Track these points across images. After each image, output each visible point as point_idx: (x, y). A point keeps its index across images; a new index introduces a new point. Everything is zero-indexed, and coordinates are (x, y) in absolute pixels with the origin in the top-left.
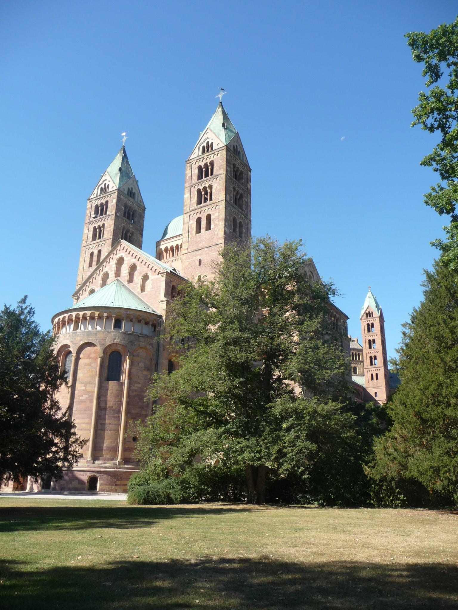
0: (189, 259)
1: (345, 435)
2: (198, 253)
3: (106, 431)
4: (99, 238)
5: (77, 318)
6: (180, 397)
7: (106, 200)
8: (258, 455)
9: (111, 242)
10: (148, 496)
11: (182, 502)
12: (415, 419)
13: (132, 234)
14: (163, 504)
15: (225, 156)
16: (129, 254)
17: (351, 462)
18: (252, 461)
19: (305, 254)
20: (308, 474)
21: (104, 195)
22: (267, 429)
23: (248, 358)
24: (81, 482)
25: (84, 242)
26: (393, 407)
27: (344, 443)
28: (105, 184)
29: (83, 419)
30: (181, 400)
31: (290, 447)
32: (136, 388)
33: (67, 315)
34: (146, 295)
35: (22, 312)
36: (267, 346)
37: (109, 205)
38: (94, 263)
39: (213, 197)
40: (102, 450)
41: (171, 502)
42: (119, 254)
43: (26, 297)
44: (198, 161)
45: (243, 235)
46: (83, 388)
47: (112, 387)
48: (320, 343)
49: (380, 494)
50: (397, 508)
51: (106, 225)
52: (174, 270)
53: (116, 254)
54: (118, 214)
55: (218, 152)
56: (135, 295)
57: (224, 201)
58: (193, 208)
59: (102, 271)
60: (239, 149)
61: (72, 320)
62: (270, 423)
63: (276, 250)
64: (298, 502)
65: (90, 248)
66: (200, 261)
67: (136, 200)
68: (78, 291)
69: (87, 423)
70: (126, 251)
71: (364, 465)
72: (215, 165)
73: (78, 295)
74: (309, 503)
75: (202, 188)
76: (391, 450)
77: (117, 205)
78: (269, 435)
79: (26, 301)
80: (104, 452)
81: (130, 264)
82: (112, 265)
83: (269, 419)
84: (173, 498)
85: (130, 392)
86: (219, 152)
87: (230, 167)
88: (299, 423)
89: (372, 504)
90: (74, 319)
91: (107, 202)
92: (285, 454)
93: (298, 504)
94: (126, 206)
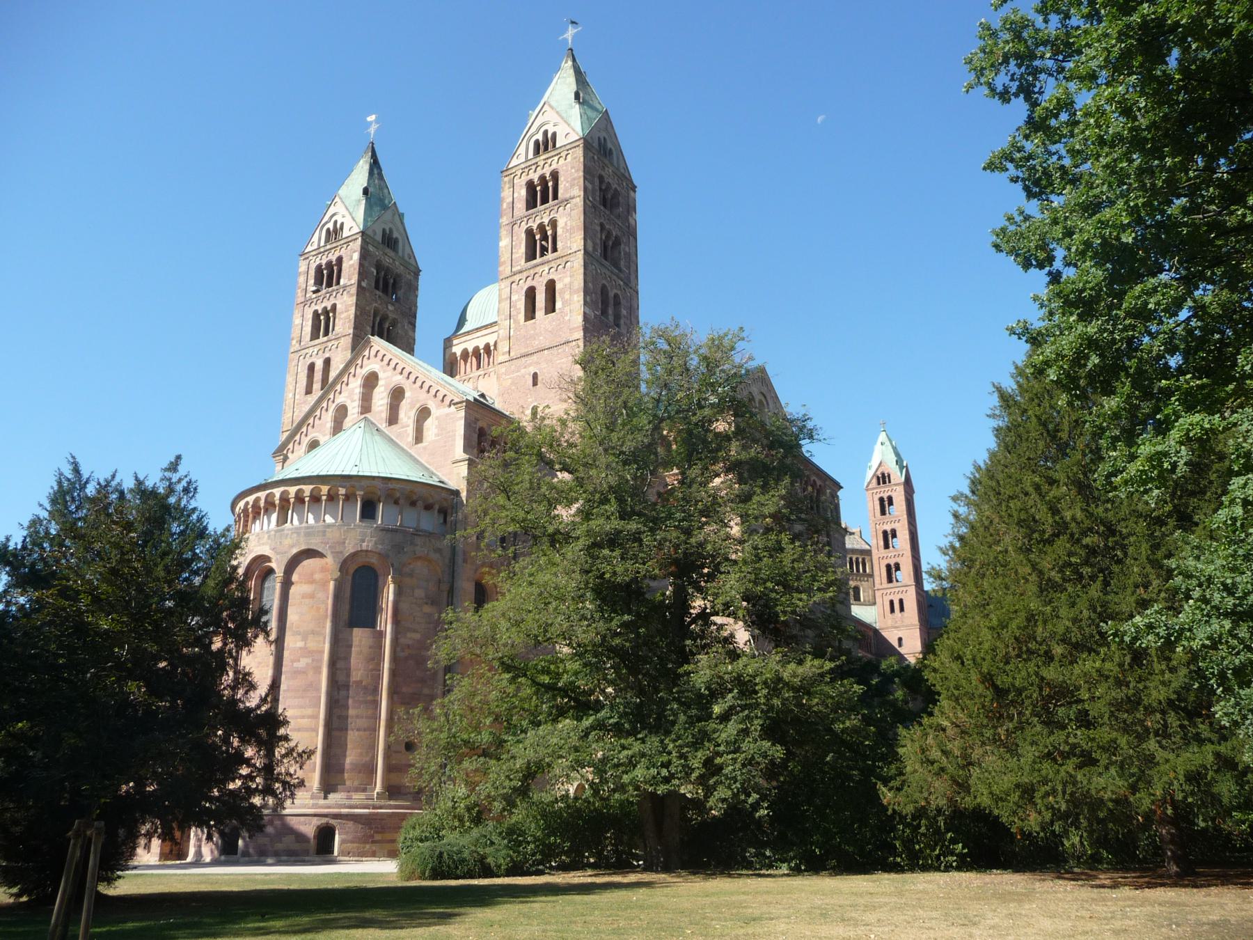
1: (841, 726)
3: (350, 732)
4: (326, 333)
5: (284, 499)
6: (502, 658)
7: (337, 254)
8: (664, 772)
9: (350, 340)
10: (440, 863)
11: (509, 873)
12: (981, 687)
13: (394, 323)
14: (472, 877)
15: (582, 159)
16: (388, 364)
17: (853, 781)
18: (651, 785)
19: (751, 358)
20: (767, 808)
21: (334, 245)
22: (682, 718)
23: (639, 573)
24: (300, 837)
25: (294, 342)
26: (936, 665)
27: (838, 741)
28: (336, 222)
29: (301, 707)
30: (503, 663)
31: (730, 753)
32: (410, 642)
33: (262, 495)
34: (425, 448)
35: (171, 490)
36: (677, 547)
37: (344, 266)
38: (317, 386)
39: (559, 245)
40: (341, 771)
41: (487, 872)
43: (179, 458)
44: (526, 170)
45: (622, 322)
46: (300, 644)
47: (360, 641)
48: (785, 538)
49: (914, 843)
50: (948, 871)
52: (483, 396)
53: (362, 367)
54: (364, 284)
56: (403, 449)
57: (582, 252)
58: (519, 268)
60: (609, 145)
61: (273, 505)
62: (686, 705)
63: (690, 350)
64: (749, 865)
66: (535, 376)
67: (400, 253)
69: (309, 717)
70: (382, 360)
71: (880, 786)
72: (561, 179)
74: (770, 867)
75: (535, 227)
76: (935, 754)
77: (361, 265)
78: (686, 729)
79: (179, 468)
82: (353, 389)
83: (685, 697)
84: (493, 864)
85: (398, 649)
87: (592, 183)
88: (746, 704)
89: (898, 864)
90: (277, 502)
91: (340, 260)
92: (720, 768)
93: (747, 869)
94: (379, 266)
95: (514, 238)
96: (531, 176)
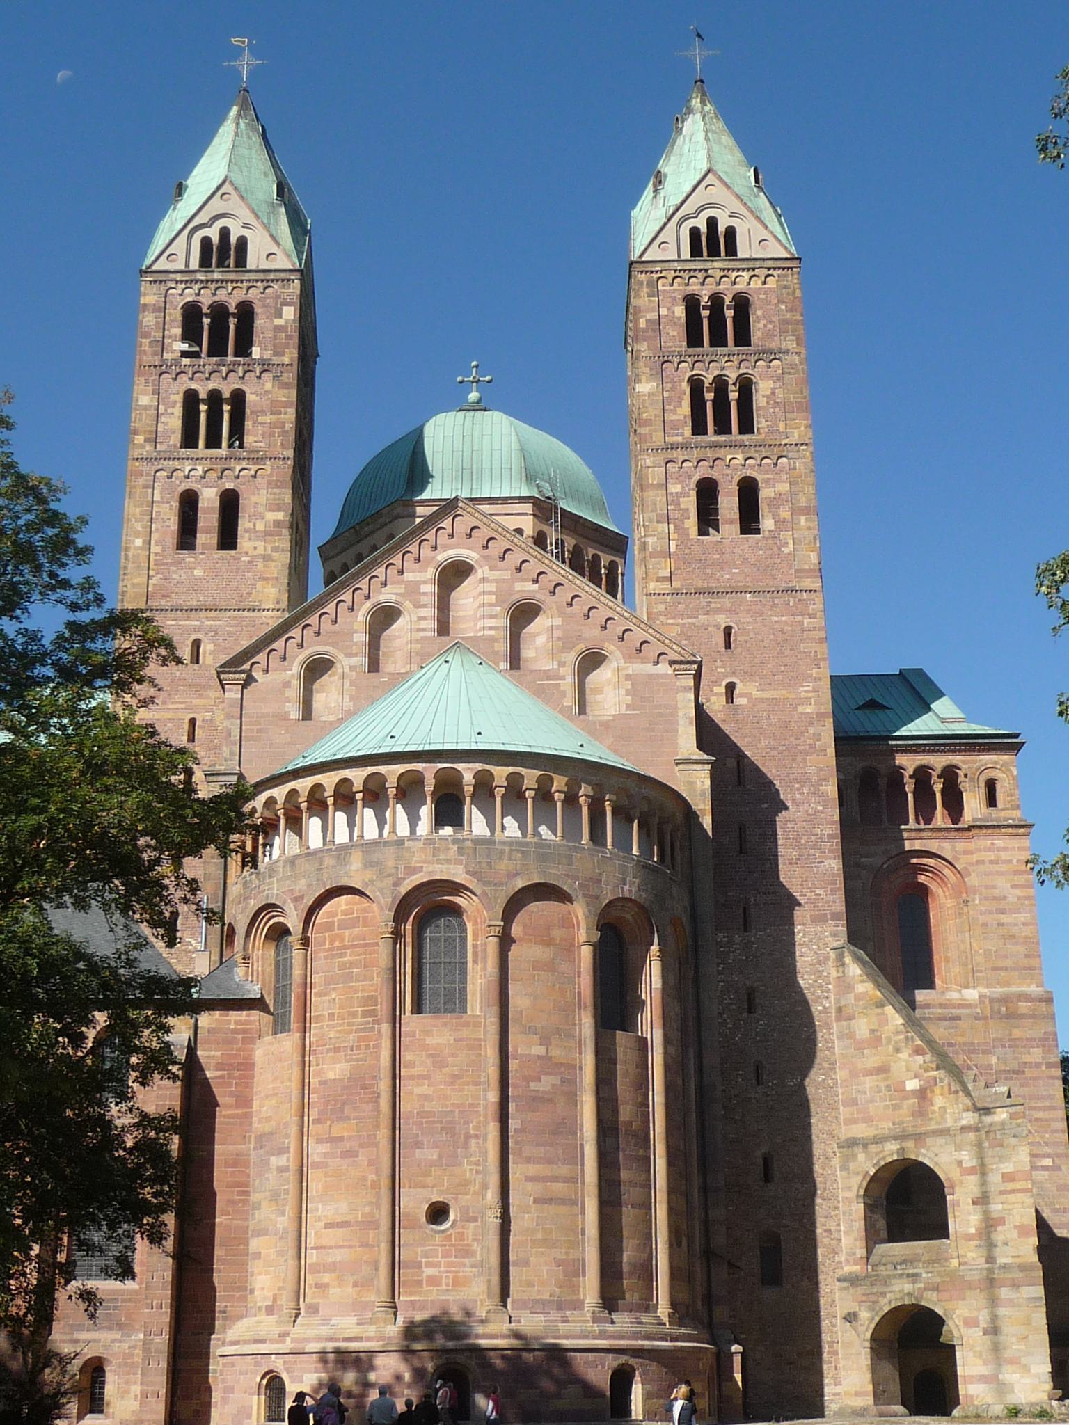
2: (716, 603)
3: (624, 1209)
21: (232, 276)
24: (588, 1390)
25: (140, 439)
28: (225, 233)
29: (549, 1161)
40: (619, 1275)
42: (446, 548)
46: (538, 1050)
47: (625, 1053)
51: (251, 398)
58: (680, 439)
59: (368, 597)
66: (728, 631)
68: (247, 654)
69: (566, 1180)
73: (246, 666)
75: (708, 379)
80: (625, 1282)
82: (417, 584)
86: (775, 273)
95: (668, 386)
96: (694, 287)
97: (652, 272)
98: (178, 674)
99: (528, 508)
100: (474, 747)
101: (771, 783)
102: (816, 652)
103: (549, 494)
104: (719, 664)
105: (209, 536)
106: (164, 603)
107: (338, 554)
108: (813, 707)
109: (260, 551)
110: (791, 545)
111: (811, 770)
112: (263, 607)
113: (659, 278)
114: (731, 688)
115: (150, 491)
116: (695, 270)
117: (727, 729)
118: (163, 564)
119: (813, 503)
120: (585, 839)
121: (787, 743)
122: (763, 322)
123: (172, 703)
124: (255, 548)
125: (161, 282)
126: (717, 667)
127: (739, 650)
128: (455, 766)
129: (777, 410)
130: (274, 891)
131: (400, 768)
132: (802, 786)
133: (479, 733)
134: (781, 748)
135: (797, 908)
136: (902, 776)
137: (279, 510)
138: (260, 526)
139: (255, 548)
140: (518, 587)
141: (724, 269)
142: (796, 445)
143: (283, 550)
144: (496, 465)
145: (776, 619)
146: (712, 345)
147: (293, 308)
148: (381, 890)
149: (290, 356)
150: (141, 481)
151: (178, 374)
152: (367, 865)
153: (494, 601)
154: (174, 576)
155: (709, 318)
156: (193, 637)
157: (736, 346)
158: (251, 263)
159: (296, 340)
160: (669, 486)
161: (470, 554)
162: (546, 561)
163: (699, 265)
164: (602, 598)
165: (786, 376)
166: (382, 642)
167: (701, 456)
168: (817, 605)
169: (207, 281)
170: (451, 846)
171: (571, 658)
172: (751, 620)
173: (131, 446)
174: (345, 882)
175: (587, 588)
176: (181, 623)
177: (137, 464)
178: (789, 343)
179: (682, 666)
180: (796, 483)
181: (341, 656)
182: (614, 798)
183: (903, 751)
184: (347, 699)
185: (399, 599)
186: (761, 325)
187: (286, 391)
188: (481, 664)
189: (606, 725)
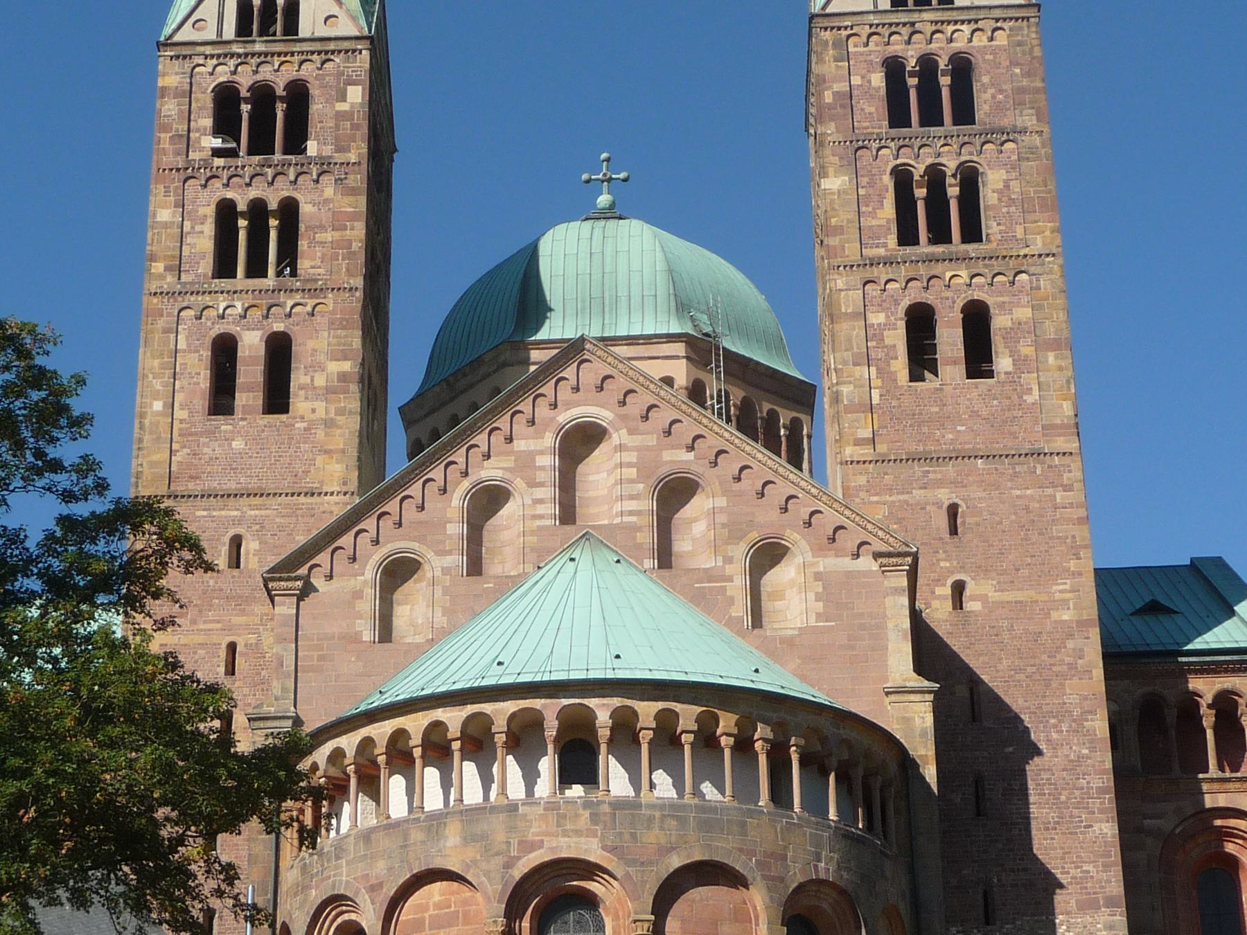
0: (890, 490)
2: (936, 472)
16: (646, 418)
25: (158, 267)
42: (569, 405)
44: (885, 31)
51: (306, 209)
53: (554, 406)
55: (993, 24)
58: (882, 251)
65: (212, 313)
66: (953, 511)
73: (303, 571)
75: (919, 170)
81: (664, 470)
82: (531, 455)
86: (1006, 25)
95: (864, 181)
96: (896, 47)
97: (839, 28)
98: (211, 582)
99: (679, 348)
100: (610, 675)
101: (1017, 719)
102: (1074, 537)
103: (708, 329)
104: (941, 555)
105: (251, 394)
106: (192, 487)
107: (426, 416)
108: (1071, 612)
109: (321, 413)
110: (1036, 392)
111: (1072, 699)
112: (324, 491)
113: (849, 37)
114: (959, 588)
115: (172, 336)
116: (897, 24)
117: (955, 644)
118: (191, 434)
119: (1065, 334)
120: (764, 799)
121: (1037, 661)
122: (991, 91)
123: (205, 622)
124: (314, 411)
125: (185, 57)
126: (938, 560)
127: (969, 536)
128: (585, 701)
129: (1013, 209)
130: (342, 878)
131: (511, 706)
132: (1060, 721)
133: (618, 657)
134: (1029, 670)
135: (1058, 891)
136: (1198, 705)
137: (345, 359)
138: (320, 381)
139: (314, 411)
140: (667, 456)
141: (936, 22)
142: (1040, 255)
143: (350, 412)
144: (636, 292)
145: (1018, 492)
146: (922, 125)
147: (360, 88)
148: (487, 874)
149: (358, 152)
150: (161, 323)
151: (208, 180)
152: (469, 839)
153: (635, 476)
154: (206, 450)
155: (919, 88)
156: (231, 533)
157: (955, 124)
158: (304, 30)
159: (365, 130)
160: (870, 316)
161: (601, 414)
162: (705, 421)
163: (903, 18)
164: (781, 470)
165: (1024, 164)
166: (485, 533)
167: (911, 274)
168: (1074, 472)
169: (246, 55)
170: (581, 811)
171: (740, 553)
172: (984, 495)
173: (146, 276)
174: (438, 863)
175: (759, 456)
176: (214, 513)
177: (155, 301)
178: (1028, 119)
179: (894, 560)
180: (1041, 307)
181: (430, 555)
182: (802, 742)
183: (1196, 672)
184: (438, 612)
185: (508, 476)
186: (987, 96)
187: (352, 199)
188: (618, 561)
189: (789, 642)
